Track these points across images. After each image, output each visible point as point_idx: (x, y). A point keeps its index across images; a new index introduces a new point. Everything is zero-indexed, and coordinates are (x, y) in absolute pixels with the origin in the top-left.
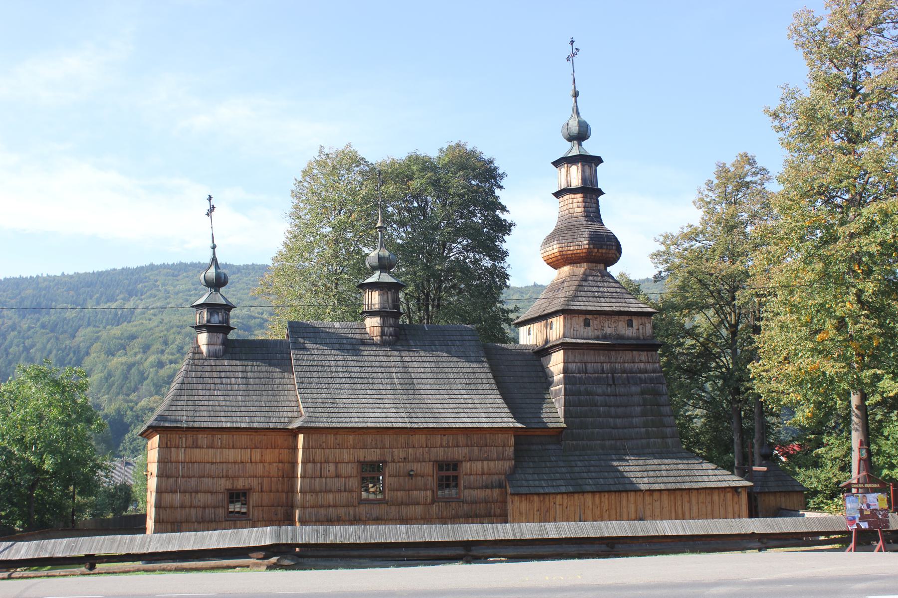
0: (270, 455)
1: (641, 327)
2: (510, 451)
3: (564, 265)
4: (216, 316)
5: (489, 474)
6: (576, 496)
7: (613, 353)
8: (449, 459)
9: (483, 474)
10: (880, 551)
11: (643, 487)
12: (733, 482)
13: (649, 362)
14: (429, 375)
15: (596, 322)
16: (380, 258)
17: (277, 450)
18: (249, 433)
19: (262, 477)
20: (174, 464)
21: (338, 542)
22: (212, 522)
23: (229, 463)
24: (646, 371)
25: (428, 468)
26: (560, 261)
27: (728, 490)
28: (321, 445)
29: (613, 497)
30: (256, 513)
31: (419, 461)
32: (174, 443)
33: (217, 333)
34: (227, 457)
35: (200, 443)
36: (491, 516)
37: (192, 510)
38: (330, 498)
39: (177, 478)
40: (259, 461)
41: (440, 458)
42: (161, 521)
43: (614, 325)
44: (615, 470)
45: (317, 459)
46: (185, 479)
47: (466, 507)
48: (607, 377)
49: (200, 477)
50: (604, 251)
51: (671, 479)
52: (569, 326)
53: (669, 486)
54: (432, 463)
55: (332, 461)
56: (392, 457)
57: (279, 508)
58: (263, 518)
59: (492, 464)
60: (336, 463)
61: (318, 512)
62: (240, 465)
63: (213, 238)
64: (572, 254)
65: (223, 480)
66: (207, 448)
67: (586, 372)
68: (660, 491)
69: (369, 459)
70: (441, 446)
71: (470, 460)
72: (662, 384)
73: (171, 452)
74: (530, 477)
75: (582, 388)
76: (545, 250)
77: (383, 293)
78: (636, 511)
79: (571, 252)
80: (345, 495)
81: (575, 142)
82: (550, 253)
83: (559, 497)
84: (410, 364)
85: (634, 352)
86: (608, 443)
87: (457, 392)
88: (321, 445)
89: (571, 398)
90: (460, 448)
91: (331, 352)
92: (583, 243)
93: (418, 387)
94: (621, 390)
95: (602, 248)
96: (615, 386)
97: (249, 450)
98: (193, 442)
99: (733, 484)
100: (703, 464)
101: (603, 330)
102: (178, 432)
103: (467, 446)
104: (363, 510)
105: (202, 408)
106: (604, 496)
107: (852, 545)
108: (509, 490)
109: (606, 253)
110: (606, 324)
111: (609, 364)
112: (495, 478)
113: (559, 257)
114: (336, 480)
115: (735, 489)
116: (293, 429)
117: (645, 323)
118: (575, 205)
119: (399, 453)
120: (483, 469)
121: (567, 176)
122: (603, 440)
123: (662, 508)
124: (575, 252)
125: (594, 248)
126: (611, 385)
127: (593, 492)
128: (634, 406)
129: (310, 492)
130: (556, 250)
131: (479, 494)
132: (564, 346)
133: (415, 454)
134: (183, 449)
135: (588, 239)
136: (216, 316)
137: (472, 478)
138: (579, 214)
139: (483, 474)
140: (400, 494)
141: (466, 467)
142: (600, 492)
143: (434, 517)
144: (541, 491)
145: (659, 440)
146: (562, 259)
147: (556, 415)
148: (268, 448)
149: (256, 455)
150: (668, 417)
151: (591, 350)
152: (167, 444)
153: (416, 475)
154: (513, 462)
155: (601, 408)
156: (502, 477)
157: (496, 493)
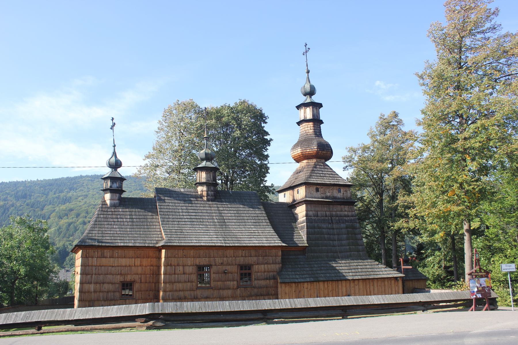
0: (145, 262)
1: (345, 192)
2: (279, 259)
3: (304, 160)
4: (115, 184)
5: (268, 272)
6: (315, 283)
7: (331, 206)
9: (265, 272)
10: (486, 310)
11: (350, 278)
12: (395, 275)
13: (349, 211)
14: (234, 218)
15: (322, 190)
16: (206, 154)
17: (149, 259)
18: (134, 249)
19: (141, 274)
20: (90, 267)
21: (190, 312)
22: (112, 300)
23: (122, 266)
24: (348, 216)
25: (234, 268)
26: (301, 158)
27: (392, 279)
28: (175, 256)
29: (334, 283)
30: (137, 295)
31: (230, 265)
32: (90, 255)
33: (116, 193)
34: (121, 263)
35: (105, 254)
36: (269, 295)
37: (101, 293)
38: (180, 286)
39: (92, 275)
40: (139, 265)
41: (241, 263)
42: (83, 300)
43: (331, 191)
44: (334, 268)
45: (173, 263)
46: (97, 276)
47: (256, 290)
48: (328, 219)
49: (105, 274)
50: (325, 152)
51: (363, 273)
52: (308, 191)
53: (363, 277)
54: (236, 266)
55: (181, 264)
56: (215, 262)
57: (151, 292)
58: (142, 297)
59: (269, 266)
60: (183, 266)
61: (173, 294)
62: (129, 268)
63: (114, 141)
65: (119, 276)
66: (109, 258)
67: (317, 216)
68: (358, 280)
70: (242, 256)
71: (258, 264)
72: (357, 223)
73: (89, 260)
74: (290, 273)
75: (316, 225)
76: (293, 152)
77: (208, 173)
78: (346, 291)
79: (307, 153)
80: (189, 284)
81: (308, 96)
82: (296, 153)
83: (306, 284)
84: (223, 212)
85: (342, 206)
86: (330, 254)
87: (249, 227)
88: (175, 256)
89: (310, 230)
90: (252, 258)
91: (179, 205)
92: (314, 148)
93: (228, 224)
95: (324, 151)
97: (134, 259)
98: (102, 254)
99: (395, 276)
100: (379, 265)
101: (326, 194)
102: (93, 249)
103: (256, 256)
104: (199, 293)
105: (107, 235)
106: (330, 283)
107: (473, 306)
108: (279, 281)
109: (326, 153)
110: (327, 191)
111: (329, 212)
112: (271, 274)
113: (301, 156)
114: (183, 275)
115: (396, 278)
116: (159, 247)
118: (309, 128)
119: (218, 260)
120: (265, 269)
121: (304, 113)
122: (328, 253)
123: (359, 289)
124: (310, 152)
125: (320, 150)
126: (331, 223)
127: (324, 281)
128: (343, 234)
129: (169, 283)
131: (263, 283)
132: (306, 202)
133: (228, 261)
134: (96, 259)
135: (317, 146)
136: (115, 184)
137: (259, 274)
138: (311, 133)
139: (265, 272)
140: (219, 283)
141: (256, 268)
142: (327, 281)
143: (238, 296)
144: (297, 281)
145: (356, 253)
147: (302, 239)
148: (144, 258)
149: (138, 262)
150: (360, 241)
151: (320, 204)
152: (86, 255)
153: (228, 273)
154: (281, 265)
155: (326, 236)
156: (275, 273)
157: (272, 282)
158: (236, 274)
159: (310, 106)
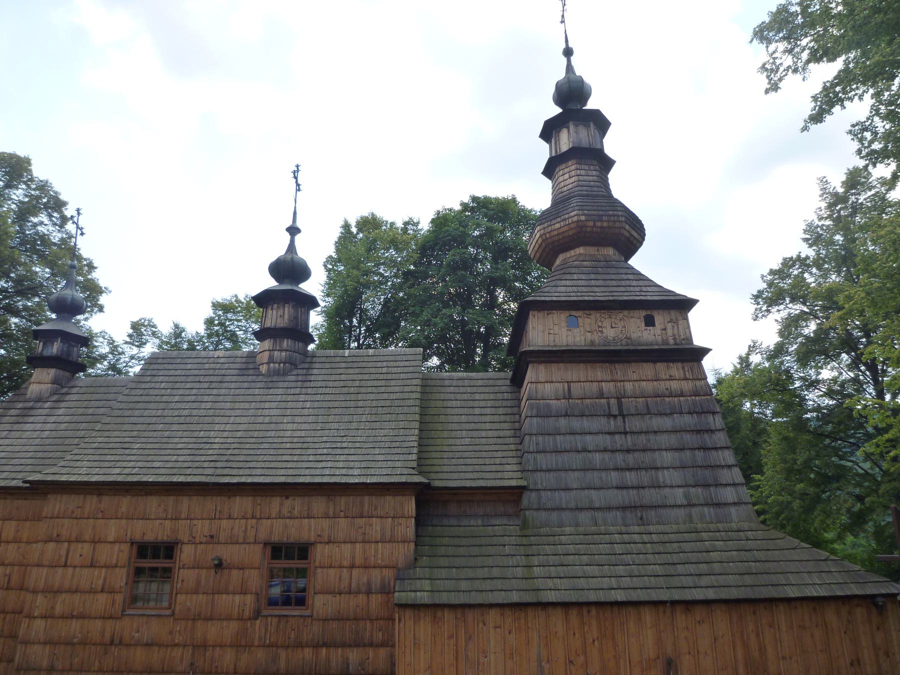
1: (669, 326)
2: (408, 528)
8: (292, 540)
9: (352, 566)
13: (686, 379)
15: (587, 321)
19: (12, 565)
25: (255, 554)
41: (275, 538)
50: (605, 224)
56: (191, 534)
64: (558, 234)
69: (150, 537)
72: (714, 413)
79: (555, 233)
80: (102, 598)
94: (635, 424)
96: (624, 418)
101: (602, 332)
106: (589, 612)
110: (607, 323)
117: (677, 320)
120: (353, 558)
124: (561, 231)
126: (615, 416)
139: (352, 566)
141: (320, 553)
143: (256, 643)
150: (725, 471)
153: (230, 568)
154: (412, 545)
156: (389, 574)
158: (254, 573)
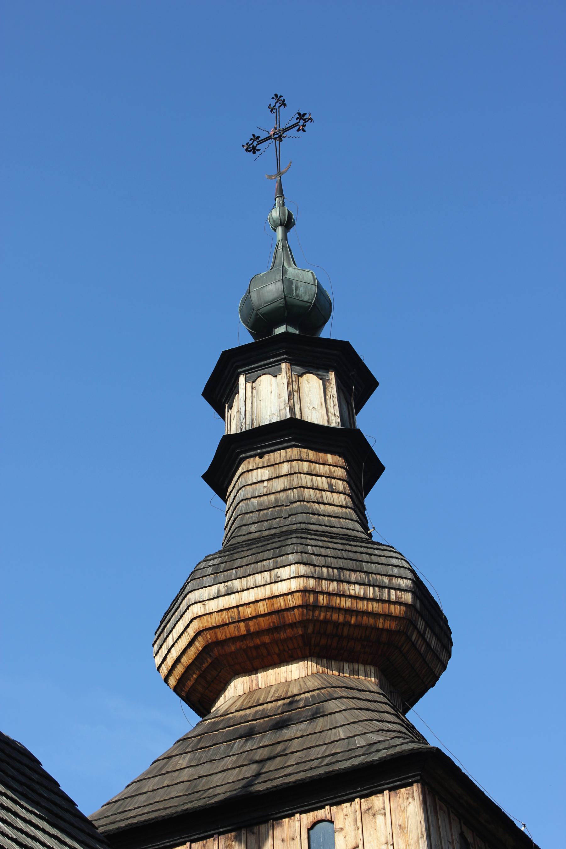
76: (222, 588)
79: (346, 603)
121: (290, 394)
124: (362, 606)
130: (294, 585)
146: (303, 623)
159: (327, 370)
